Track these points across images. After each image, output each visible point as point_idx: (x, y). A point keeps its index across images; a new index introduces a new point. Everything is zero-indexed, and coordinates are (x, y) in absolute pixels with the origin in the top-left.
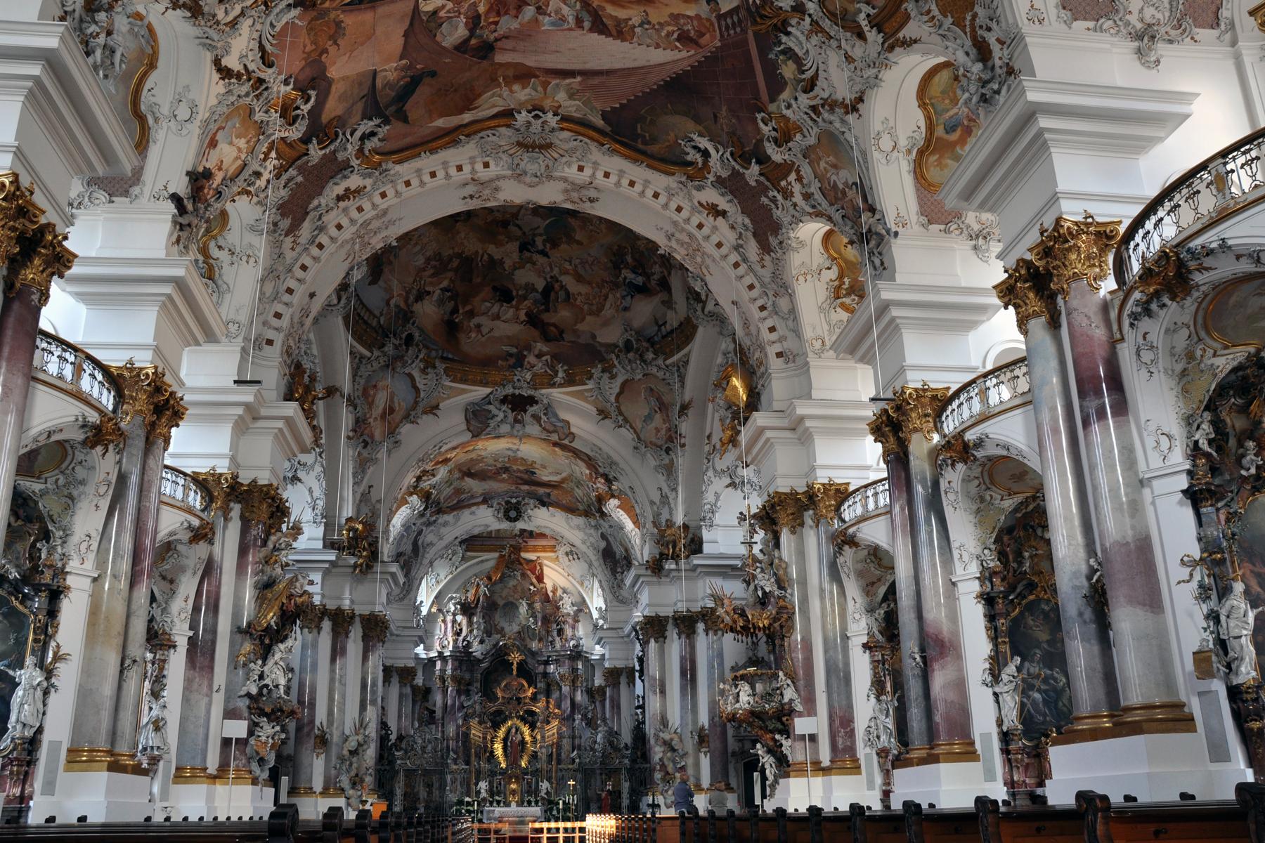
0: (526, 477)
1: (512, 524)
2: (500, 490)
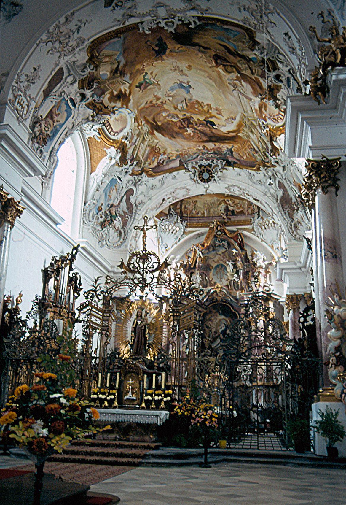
0: (207, 130)
1: (206, 186)
2: (191, 152)
